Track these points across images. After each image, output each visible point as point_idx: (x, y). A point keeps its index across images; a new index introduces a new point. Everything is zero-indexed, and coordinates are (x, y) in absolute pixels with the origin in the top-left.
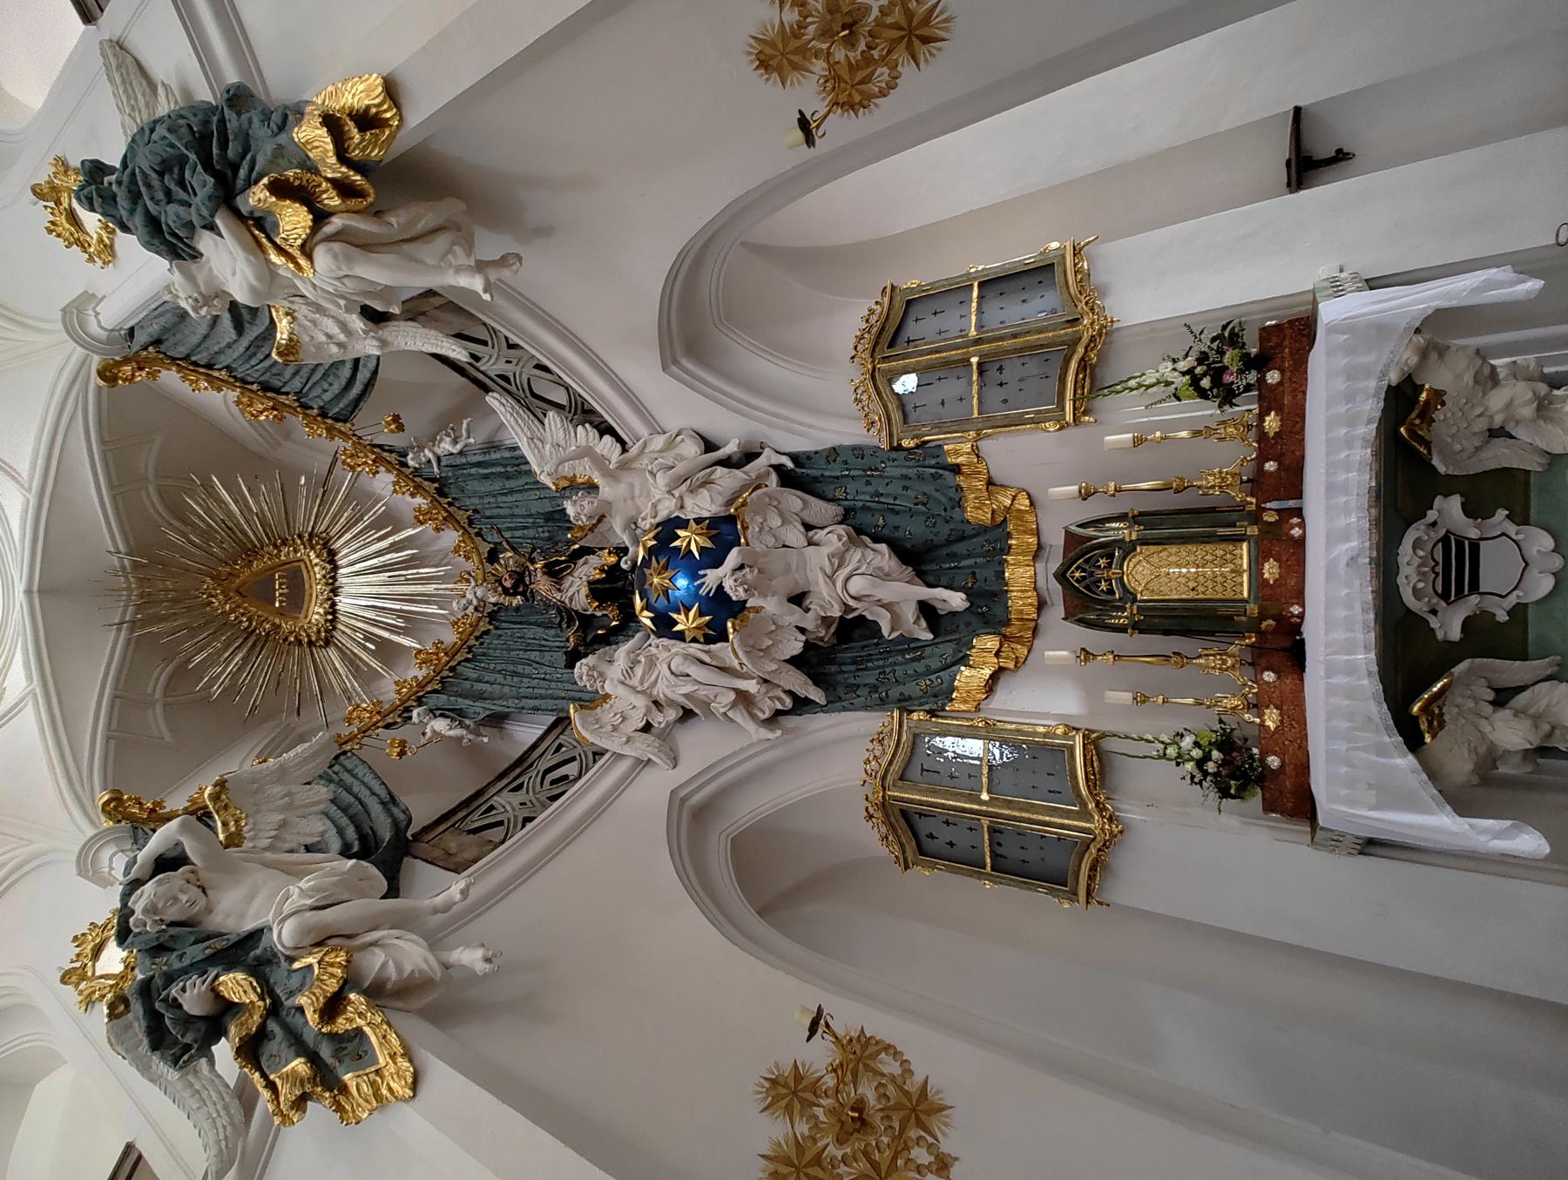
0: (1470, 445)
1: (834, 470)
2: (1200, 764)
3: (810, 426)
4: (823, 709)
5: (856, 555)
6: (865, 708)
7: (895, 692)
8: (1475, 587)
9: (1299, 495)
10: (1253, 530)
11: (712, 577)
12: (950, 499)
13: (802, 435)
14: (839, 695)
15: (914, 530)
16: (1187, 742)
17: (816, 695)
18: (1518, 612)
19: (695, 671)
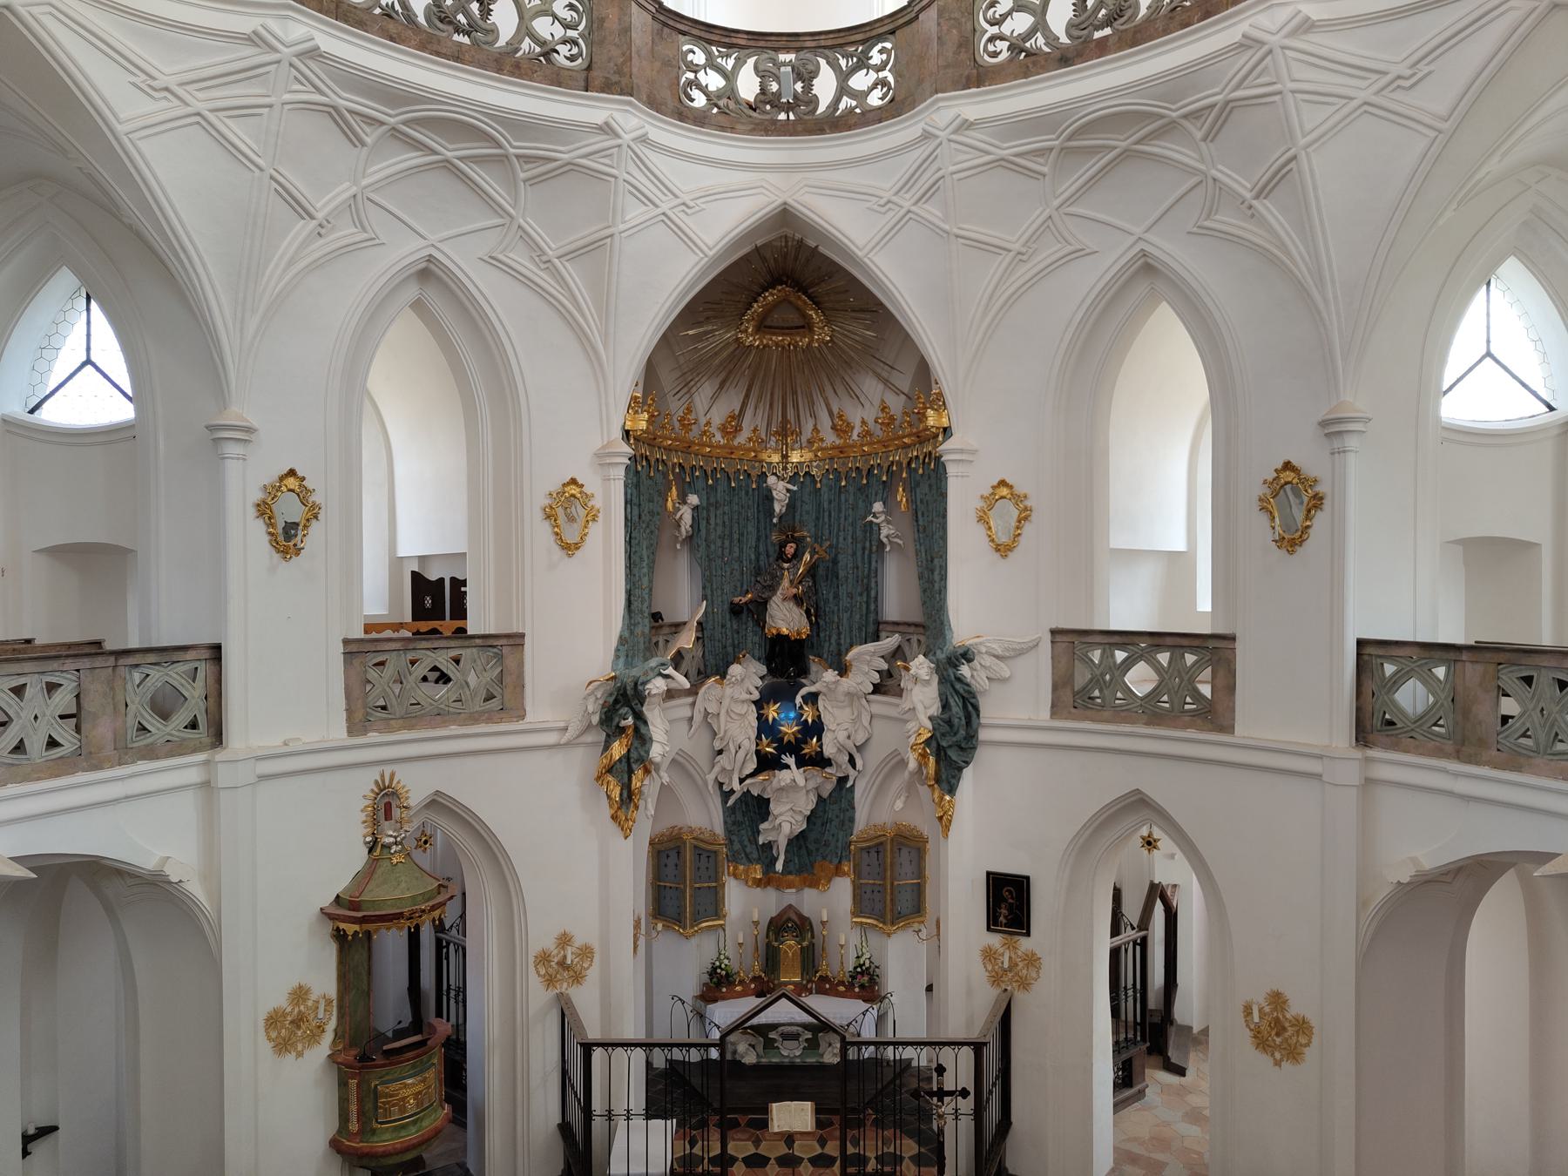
0: (828, 1040)
1: (844, 805)
2: (720, 967)
3: (866, 798)
4: (725, 802)
5: (800, 818)
6: (725, 822)
7: (734, 838)
8: (784, 1040)
9: (816, 993)
10: (805, 982)
11: (790, 760)
12: (827, 855)
13: (862, 795)
14: (729, 812)
15: (812, 836)
16: (726, 962)
17: (730, 803)
18: (778, 1048)
19: (741, 754)
